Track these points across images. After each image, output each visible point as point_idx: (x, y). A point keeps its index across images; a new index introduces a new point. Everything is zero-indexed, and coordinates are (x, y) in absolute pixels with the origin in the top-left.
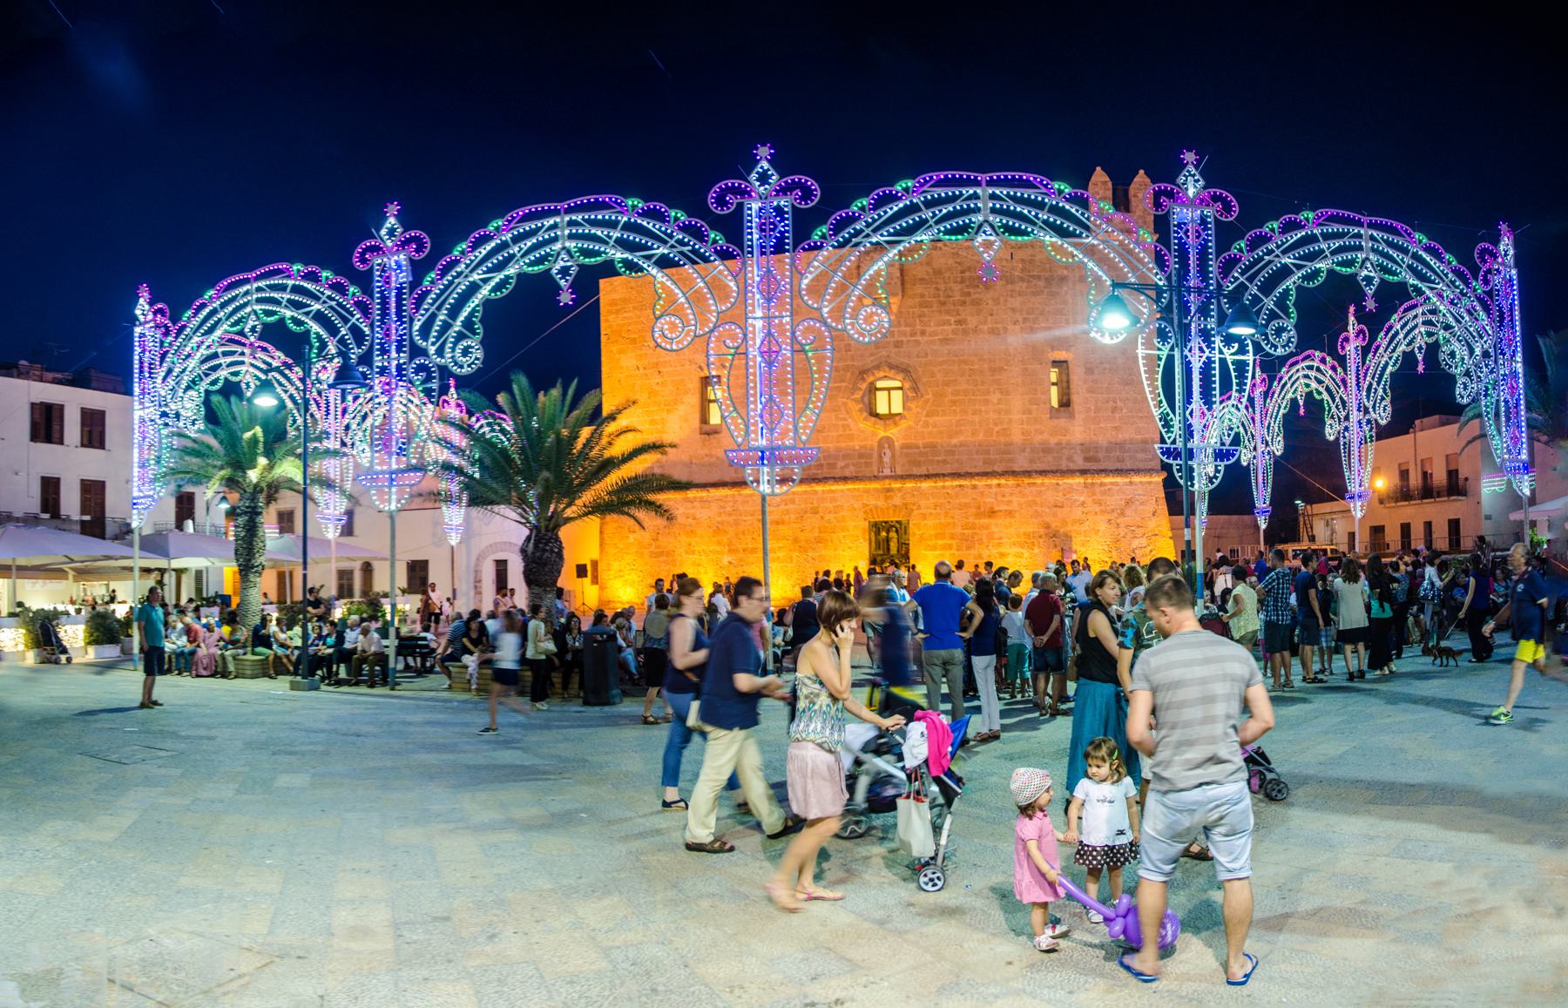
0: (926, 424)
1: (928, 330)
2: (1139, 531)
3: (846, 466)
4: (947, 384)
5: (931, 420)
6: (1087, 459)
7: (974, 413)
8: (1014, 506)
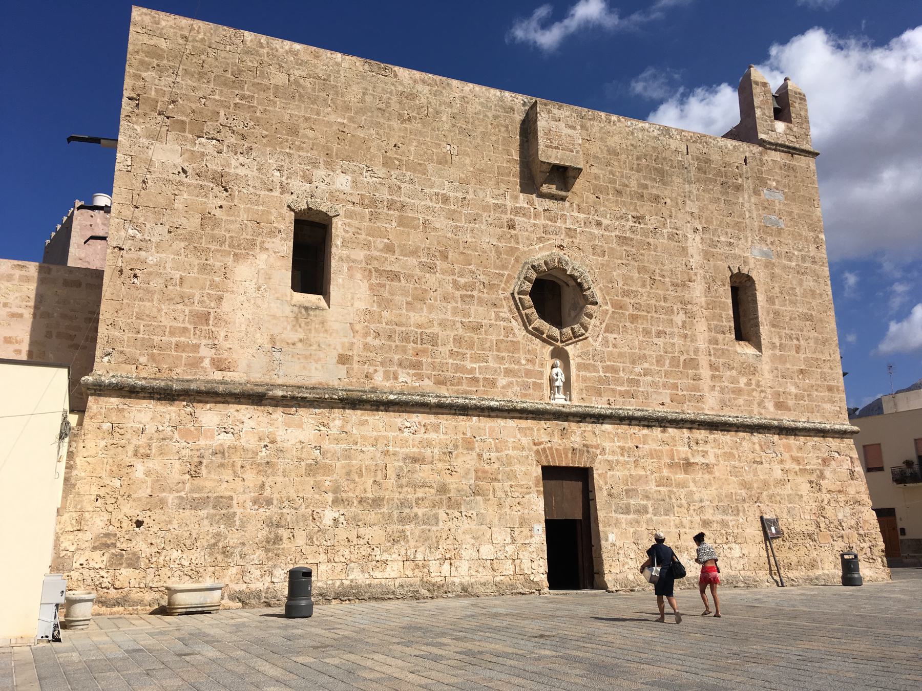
0: (606, 342)
1: (605, 222)
2: (842, 498)
3: (510, 385)
4: (627, 293)
5: (611, 337)
6: (779, 406)
7: (659, 334)
8: (711, 459)
